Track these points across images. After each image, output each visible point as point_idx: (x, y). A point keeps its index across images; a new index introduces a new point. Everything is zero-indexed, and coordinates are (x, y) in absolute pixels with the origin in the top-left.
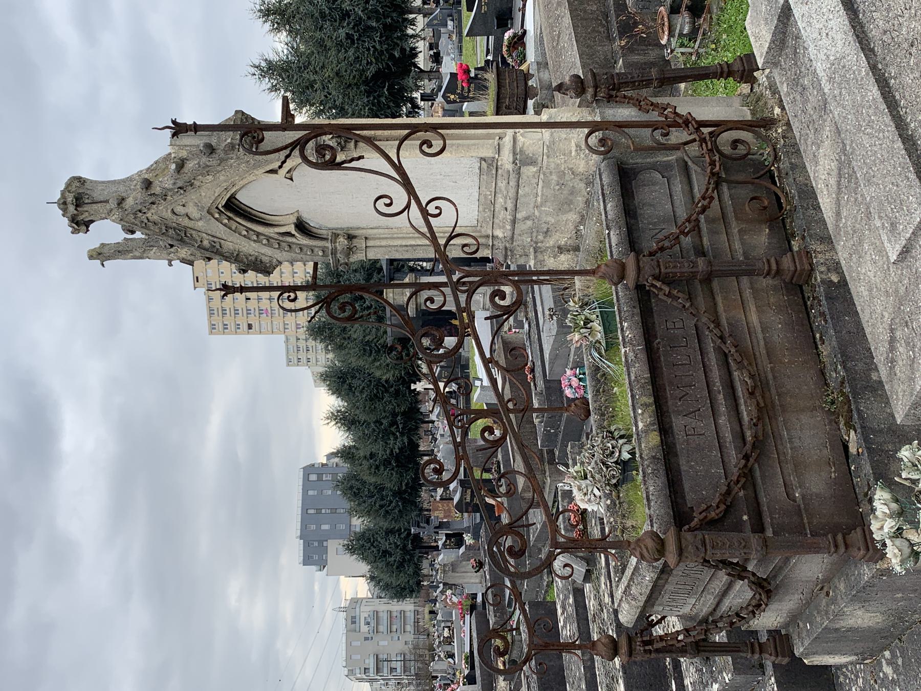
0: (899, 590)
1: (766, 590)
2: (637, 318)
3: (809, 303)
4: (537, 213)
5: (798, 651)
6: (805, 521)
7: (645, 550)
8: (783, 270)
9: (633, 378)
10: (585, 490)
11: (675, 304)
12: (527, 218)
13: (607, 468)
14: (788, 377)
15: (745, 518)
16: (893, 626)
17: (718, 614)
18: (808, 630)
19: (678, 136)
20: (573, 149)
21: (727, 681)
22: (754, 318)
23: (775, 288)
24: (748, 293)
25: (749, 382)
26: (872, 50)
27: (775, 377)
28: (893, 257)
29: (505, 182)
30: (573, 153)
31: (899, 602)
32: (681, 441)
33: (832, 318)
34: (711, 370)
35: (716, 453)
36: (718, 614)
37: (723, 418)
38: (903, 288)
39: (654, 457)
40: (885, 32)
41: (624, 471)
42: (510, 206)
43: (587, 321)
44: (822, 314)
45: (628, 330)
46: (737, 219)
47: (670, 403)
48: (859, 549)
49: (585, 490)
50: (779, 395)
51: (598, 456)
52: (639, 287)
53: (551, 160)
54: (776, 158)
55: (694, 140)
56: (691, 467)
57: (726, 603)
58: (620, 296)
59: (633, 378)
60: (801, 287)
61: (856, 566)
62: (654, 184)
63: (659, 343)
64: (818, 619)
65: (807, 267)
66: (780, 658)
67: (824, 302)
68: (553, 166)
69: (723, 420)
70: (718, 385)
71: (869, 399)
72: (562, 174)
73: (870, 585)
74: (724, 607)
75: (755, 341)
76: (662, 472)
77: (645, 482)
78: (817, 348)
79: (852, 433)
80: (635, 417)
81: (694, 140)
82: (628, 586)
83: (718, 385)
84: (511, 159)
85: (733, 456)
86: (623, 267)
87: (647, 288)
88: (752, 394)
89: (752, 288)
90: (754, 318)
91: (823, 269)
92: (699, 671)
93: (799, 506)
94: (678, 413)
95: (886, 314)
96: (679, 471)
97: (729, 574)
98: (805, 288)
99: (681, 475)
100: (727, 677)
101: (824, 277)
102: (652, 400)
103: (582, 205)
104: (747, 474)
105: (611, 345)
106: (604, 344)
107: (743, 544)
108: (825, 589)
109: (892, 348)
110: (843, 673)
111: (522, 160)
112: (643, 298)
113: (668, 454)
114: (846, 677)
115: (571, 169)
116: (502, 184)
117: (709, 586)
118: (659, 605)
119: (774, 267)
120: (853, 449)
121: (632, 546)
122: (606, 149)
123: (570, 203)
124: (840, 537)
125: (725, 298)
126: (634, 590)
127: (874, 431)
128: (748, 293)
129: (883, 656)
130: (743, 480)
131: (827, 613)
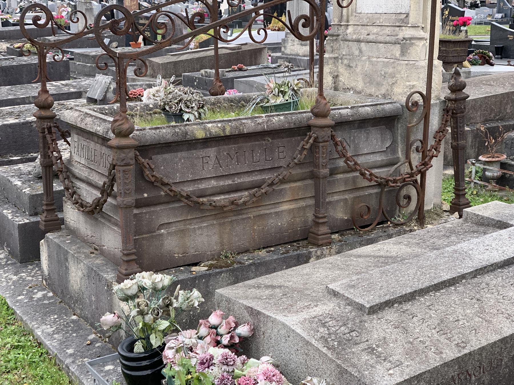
0: (97, 297)
1: (93, 211)
2: (287, 126)
3: (295, 244)
4: (364, 58)
5: (49, 235)
6: (144, 236)
7: (120, 123)
8: (319, 227)
9: (243, 121)
10: (157, 95)
11: (297, 152)
12: (361, 51)
13: (177, 103)
14: (244, 228)
15: (146, 195)
16: (71, 297)
17: (74, 181)
18: (65, 241)
19: (416, 158)
20: (411, 83)
21: (24, 191)
22: (285, 207)
23: (306, 222)
24: (302, 203)
26: (475, 277)
27: (243, 219)
28: (331, 286)
29: (389, 33)
30: (408, 83)
32: (199, 153)
33: (285, 258)
34: (249, 176)
35: (190, 177)
36: (74, 181)
37: (215, 183)
38: (309, 293)
39: (186, 133)
40: (487, 284)
42: (371, 37)
43: (284, 93)
45: (278, 120)
46: (355, 198)
47: (225, 147)
48: (126, 270)
49: (157, 95)
50: (231, 221)
51: (185, 97)
53: (404, 67)
54: (396, 225)
55: (412, 169)
56: (180, 160)
58: (304, 113)
59: (243, 121)
60: (306, 239)
61: (113, 270)
62: (383, 141)
63: (269, 141)
64: (74, 247)
65: (320, 242)
66: (44, 223)
67: (296, 253)
68: (399, 68)
69: (213, 183)
70: (238, 180)
71: (229, 279)
72: (392, 76)
73: (100, 279)
74: (79, 184)
75: (270, 207)
76: (176, 139)
77: (169, 127)
78: (264, 248)
79: (206, 268)
80: (215, 122)
81: (412, 169)
82: (91, 116)
83: (238, 180)
84: (406, 36)
85: (189, 189)
86: (324, 115)
87: (308, 133)
88: (232, 203)
89: (307, 206)
90: (285, 207)
91: (319, 253)
92: (29, 173)
93: (155, 232)
94: (219, 152)
95: (291, 283)
96: (177, 151)
97: (105, 183)
98: (305, 242)
99: (174, 152)
101: (313, 253)
102: (228, 133)
103: (368, 92)
104: (175, 198)
105: (265, 109)
106: (267, 105)
107: (127, 192)
108: (95, 252)
109: (267, 287)
110: (34, 268)
111: (405, 45)
112: (301, 130)
114: (32, 270)
115: (396, 82)
116: (388, 31)
118: (78, 138)
119: (321, 221)
120: (194, 269)
121: (122, 114)
122: (410, 107)
123: (371, 83)
124: (134, 257)
125: (299, 188)
126: (88, 120)
127: (207, 282)
128: (302, 203)
129: (49, 292)
130: (172, 194)
131: (79, 253)
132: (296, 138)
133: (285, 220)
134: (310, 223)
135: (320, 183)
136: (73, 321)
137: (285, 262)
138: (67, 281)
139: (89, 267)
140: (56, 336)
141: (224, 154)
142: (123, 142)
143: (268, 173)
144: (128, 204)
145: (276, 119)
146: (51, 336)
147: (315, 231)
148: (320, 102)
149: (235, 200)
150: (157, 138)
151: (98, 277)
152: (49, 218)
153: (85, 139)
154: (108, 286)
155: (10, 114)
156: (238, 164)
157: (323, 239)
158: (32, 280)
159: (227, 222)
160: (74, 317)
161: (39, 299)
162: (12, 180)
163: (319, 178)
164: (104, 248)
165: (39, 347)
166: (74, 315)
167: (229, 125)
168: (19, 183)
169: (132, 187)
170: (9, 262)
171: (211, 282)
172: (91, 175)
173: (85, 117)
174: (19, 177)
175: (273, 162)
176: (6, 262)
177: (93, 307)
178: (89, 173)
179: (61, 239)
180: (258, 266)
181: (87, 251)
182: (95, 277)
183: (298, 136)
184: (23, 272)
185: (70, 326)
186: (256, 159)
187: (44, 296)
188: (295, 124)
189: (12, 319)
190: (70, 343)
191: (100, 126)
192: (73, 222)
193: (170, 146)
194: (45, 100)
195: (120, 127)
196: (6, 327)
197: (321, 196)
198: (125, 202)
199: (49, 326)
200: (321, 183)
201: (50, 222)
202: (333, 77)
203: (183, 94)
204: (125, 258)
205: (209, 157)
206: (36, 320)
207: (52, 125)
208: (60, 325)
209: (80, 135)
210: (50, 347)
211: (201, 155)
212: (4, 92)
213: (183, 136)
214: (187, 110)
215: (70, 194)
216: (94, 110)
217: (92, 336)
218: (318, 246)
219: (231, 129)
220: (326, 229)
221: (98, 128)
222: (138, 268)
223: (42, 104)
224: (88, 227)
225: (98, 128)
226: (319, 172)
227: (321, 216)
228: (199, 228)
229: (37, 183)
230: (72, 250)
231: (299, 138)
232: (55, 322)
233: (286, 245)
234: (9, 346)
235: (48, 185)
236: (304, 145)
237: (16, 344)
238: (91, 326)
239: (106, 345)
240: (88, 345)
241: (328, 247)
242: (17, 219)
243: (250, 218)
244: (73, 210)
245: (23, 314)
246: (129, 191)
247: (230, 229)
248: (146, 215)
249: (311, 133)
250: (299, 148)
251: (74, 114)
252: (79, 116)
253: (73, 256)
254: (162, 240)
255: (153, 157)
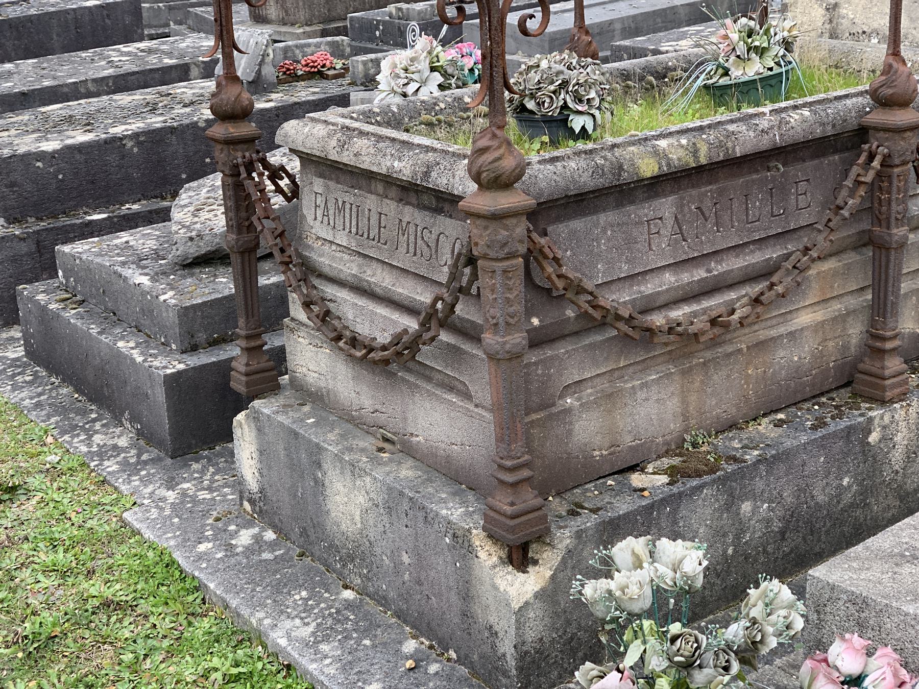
0: (419, 557)
2: (819, 132)
3: (824, 399)
6: (534, 416)
7: (496, 154)
8: (882, 359)
9: (731, 128)
10: (412, 69)
11: (844, 193)
13: (554, 92)
14: (728, 376)
16: (331, 546)
17: (316, 282)
18: (302, 420)
21: (162, 298)
22: (805, 319)
23: (845, 347)
24: (837, 307)
25: (736, 317)
27: (728, 355)
31: (392, 558)
32: (641, 212)
33: (823, 438)
34: (737, 256)
35: (625, 269)
37: (673, 279)
39: (621, 167)
41: (548, 121)
43: (761, 52)
44: (820, 424)
47: (694, 192)
49: (412, 69)
50: (704, 364)
51: (574, 76)
52: (862, 133)
56: (604, 231)
57: (342, 294)
59: (731, 128)
60: (848, 384)
61: (455, 494)
63: (778, 169)
64: (331, 436)
65: (889, 394)
66: (244, 378)
67: (843, 423)
69: (669, 279)
70: (719, 268)
71: (717, 500)
73: (429, 519)
74: (330, 290)
75: (774, 322)
76: (601, 182)
77: (578, 153)
78: (765, 415)
79: (664, 479)
80: (671, 134)
82: (362, 133)
83: (719, 268)
85: (621, 298)
87: (866, 147)
88: (713, 322)
89: (848, 314)
90: (805, 319)
91: (887, 419)
92: (157, 255)
93: (554, 405)
94: (680, 207)
98: (845, 393)
99: (591, 214)
100: (168, 296)
101: (876, 421)
102: (703, 161)
104: (598, 319)
105: (717, 94)
106: (724, 81)
107: (511, 321)
108: (386, 446)
112: (851, 139)
113: (622, 192)
114: (203, 472)
117: (374, 264)
118: (327, 187)
119: (889, 345)
120: (636, 479)
121: (498, 132)
124: (526, 473)
125: (835, 273)
126: (360, 144)
127: (675, 511)
128: (837, 307)
129: (263, 530)
130: (597, 315)
131: (350, 449)
132: (831, 158)
133: (806, 349)
134: (853, 350)
135: (888, 261)
136: (349, 605)
137: (823, 447)
138: (321, 511)
139: (390, 489)
140: (324, 647)
141: (690, 210)
142: (503, 201)
143: (775, 245)
144: (514, 350)
145: (797, 117)
146: (312, 645)
147: (874, 370)
148: (896, 72)
149: (719, 317)
150: (562, 184)
151: (421, 515)
152: (255, 366)
153: (346, 189)
154: (455, 536)
155: (70, 120)
156: (718, 231)
157: (894, 386)
158: (213, 499)
159: (696, 365)
160: (348, 594)
161: (249, 551)
162: (127, 272)
163: (888, 249)
164: (414, 439)
165: (288, 675)
166: (346, 587)
167: (703, 140)
168: (145, 280)
169: (518, 308)
170: (145, 457)
171: (683, 512)
172: (369, 272)
173: (350, 138)
174: (139, 267)
175: (786, 218)
176: (139, 456)
177: (407, 577)
178: (360, 266)
179: (291, 414)
180: (773, 463)
181: (369, 443)
182: (411, 513)
183: (834, 153)
184: (185, 480)
185: (347, 619)
186: (754, 215)
187: (258, 539)
188: (834, 126)
189: (198, 601)
190: (364, 666)
191: (400, 159)
192: (316, 375)
193: (582, 200)
194: (236, 99)
195: (496, 164)
196: (190, 624)
197: (890, 289)
198: (508, 347)
199: (298, 622)
200: (892, 258)
201: (258, 376)
202: (828, 9)
203: (566, 71)
204: (509, 478)
205: (660, 219)
206: (263, 605)
207: (254, 156)
208: (324, 618)
209: (330, 179)
210: (322, 678)
211: (646, 215)
212: (24, 74)
213: (613, 174)
214: (580, 108)
215: (317, 316)
216: (352, 118)
217: (410, 646)
218: (883, 402)
219: (709, 149)
220: (898, 363)
221: (396, 164)
222: (536, 497)
223: (229, 108)
224: (364, 389)
225: (396, 164)
226: (890, 235)
227: (889, 334)
228: (645, 385)
229: (184, 277)
230: (330, 441)
231: (837, 157)
232: (308, 610)
233: (806, 405)
234: (218, 675)
235: (249, 293)
236: (859, 175)
237: (235, 671)
238: (399, 617)
239: (453, 669)
240: (411, 669)
241: (904, 404)
242: (156, 363)
243: (740, 351)
244: (313, 349)
245: (227, 591)
246: (516, 319)
247: (702, 382)
248: (537, 369)
249: (874, 147)
250: (849, 183)
251: (315, 131)
252: (329, 136)
253: (338, 458)
254: (571, 423)
255: (550, 229)
